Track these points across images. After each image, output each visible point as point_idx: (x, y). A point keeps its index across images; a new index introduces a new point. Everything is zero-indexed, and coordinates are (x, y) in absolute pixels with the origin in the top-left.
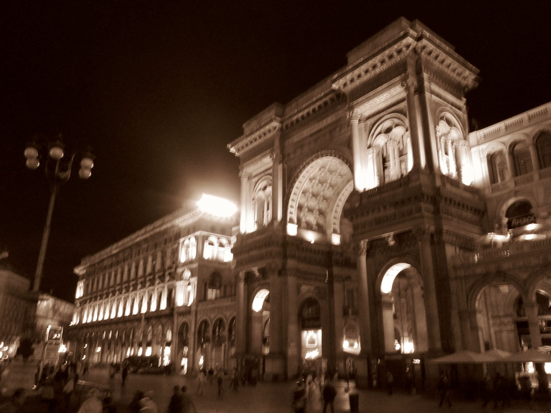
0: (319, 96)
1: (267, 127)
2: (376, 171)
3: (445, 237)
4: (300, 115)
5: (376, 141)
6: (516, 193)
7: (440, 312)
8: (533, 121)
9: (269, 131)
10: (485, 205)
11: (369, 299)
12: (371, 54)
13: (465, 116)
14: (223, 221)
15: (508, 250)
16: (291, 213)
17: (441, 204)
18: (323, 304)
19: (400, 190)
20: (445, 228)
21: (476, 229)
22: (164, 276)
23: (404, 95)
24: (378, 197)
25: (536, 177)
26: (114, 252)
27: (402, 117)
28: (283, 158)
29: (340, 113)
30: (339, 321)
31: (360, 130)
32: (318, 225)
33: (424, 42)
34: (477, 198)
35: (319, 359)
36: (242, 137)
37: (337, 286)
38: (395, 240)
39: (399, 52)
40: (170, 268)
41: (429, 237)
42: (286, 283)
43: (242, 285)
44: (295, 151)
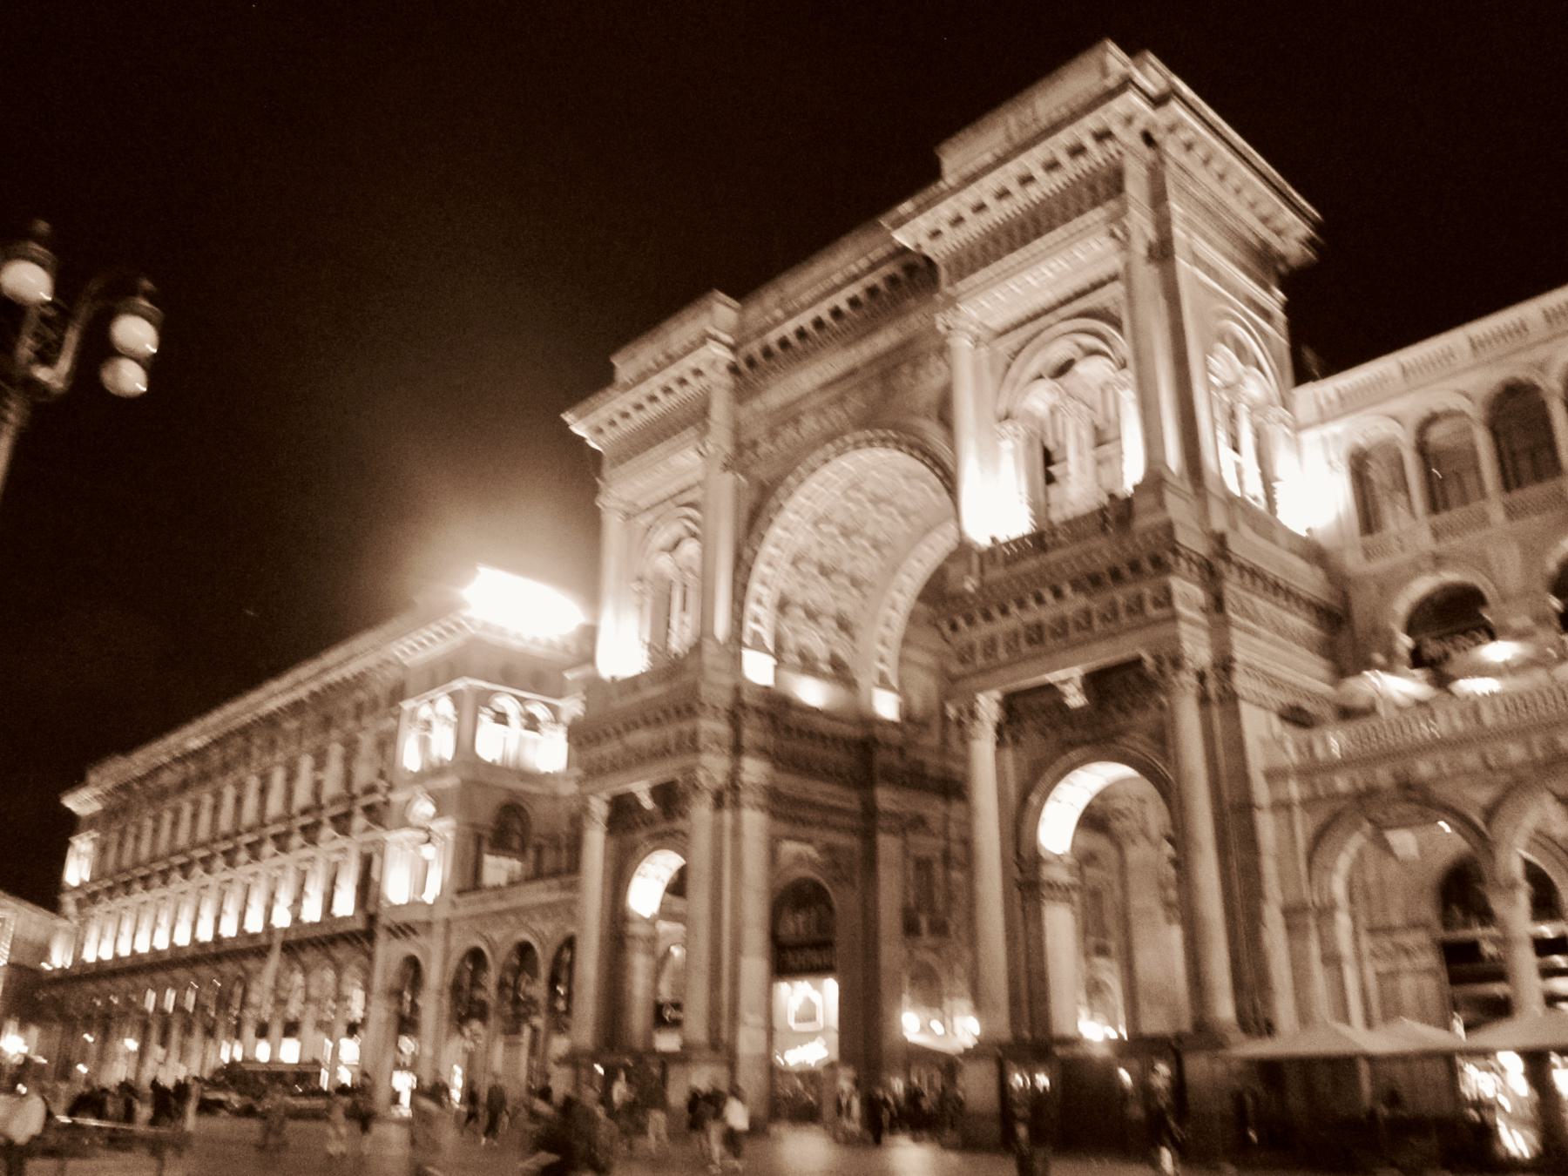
0: (854, 269)
1: (690, 362)
3: (1241, 682)
6: (1438, 561)
10: (1346, 599)
13: (1282, 341)
14: (539, 651)
16: (757, 620)
18: (844, 900)
20: (1240, 653)
22: (348, 815)
23: (1115, 263)
24: (1031, 564)
25: (1497, 513)
26: (194, 744)
29: (914, 322)
30: (891, 951)
31: (977, 368)
33: (1175, 107)
35: (831, 1066)
36: (609, 391)
37: (888, 845)
39: (1103, 136)
40: (371, 790)
41: (1193, 680)
42: (737, 833)
43: (596, 841)
44: (773, 434)
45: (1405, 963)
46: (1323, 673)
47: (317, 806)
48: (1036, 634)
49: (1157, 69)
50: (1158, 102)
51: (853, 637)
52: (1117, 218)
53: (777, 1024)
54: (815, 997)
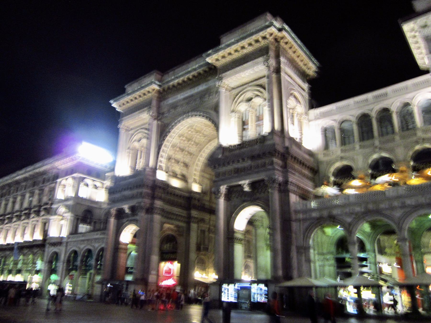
1: (147, 89)
3: (291, 187)
4: (176, 81)
5: (238, 107)
6: (342, 158)
10: (318, 167)
11: (224, 233)
16: (161, 162)
18: (181, 240)
20: (290, 179)
24: (237, 152)
25: (357, 146)
27: (262, 90)
28: (159, 116)
29: (211, 83)
30: (193, 255)
33: (284, 33)
34: (312, 159)
35: (174, 286)
36: (123, 95)
37: (194, 226)
40: (47, 204)
42: (152, 221)
43: (112, 221)
44: (169, 111)
45: (327, 263)
47: (12, 213)
50: (280, 30)
52: (267, 60)
53: (160, 274)
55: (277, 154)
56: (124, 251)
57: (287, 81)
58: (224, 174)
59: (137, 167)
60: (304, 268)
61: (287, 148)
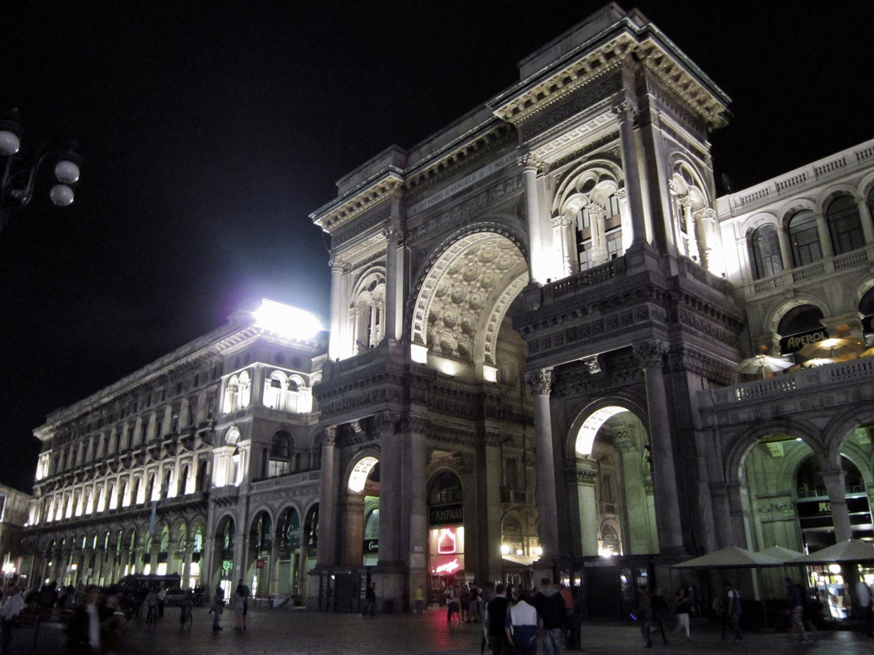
2: (566, 254)
3: (687, 360)
7: (680, 488)
8: (823, 178)
9: (383, 190)
12: (562, 58)
14: (296, 346)
15: (794, 380)
16: (418, 328)
17: (679, 307)
18: (467, 482)
19: (610, 282)
20: (687, 345)
21: (730, 351)
22: (192, 438)
23: (617, 126)
24: (572, 294)
25: (829, 267)
26: (106, 400)
27: (613, 164)
29: (505, 160)
30: (494, 511)
31: (539, 187)
32: (460, 349)
33: (651, 41)
35: (459, 573)
36: (335, 201)
37: (492, 452)
38: (601, 369)
39: (610, 56)
40: (204, 425)
41: (660, 359)
42: (407, 445)
43: (330, 449)
44: (426, 224)
45: (777, 515)
46: (731, 355)
48: (573, 335)
49: (641, 19)
51: (472, 337)
52: (618, 102)
53: (432, 552)
54: (452, 536)
55: (654, 294)
56: (359, 509)
57: (665, 139)
58: (547, 342)
59: (372, 341)
60: (729, 529)
61: (675, 280)
